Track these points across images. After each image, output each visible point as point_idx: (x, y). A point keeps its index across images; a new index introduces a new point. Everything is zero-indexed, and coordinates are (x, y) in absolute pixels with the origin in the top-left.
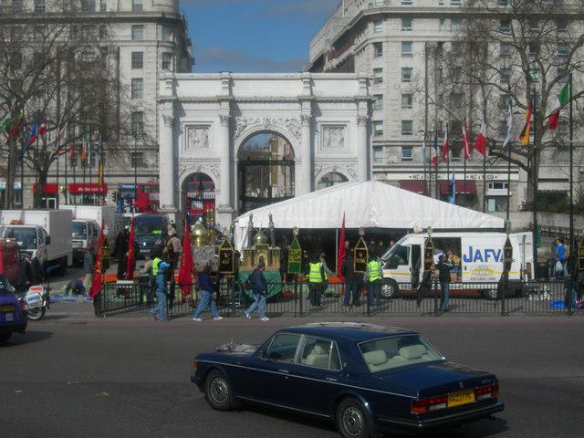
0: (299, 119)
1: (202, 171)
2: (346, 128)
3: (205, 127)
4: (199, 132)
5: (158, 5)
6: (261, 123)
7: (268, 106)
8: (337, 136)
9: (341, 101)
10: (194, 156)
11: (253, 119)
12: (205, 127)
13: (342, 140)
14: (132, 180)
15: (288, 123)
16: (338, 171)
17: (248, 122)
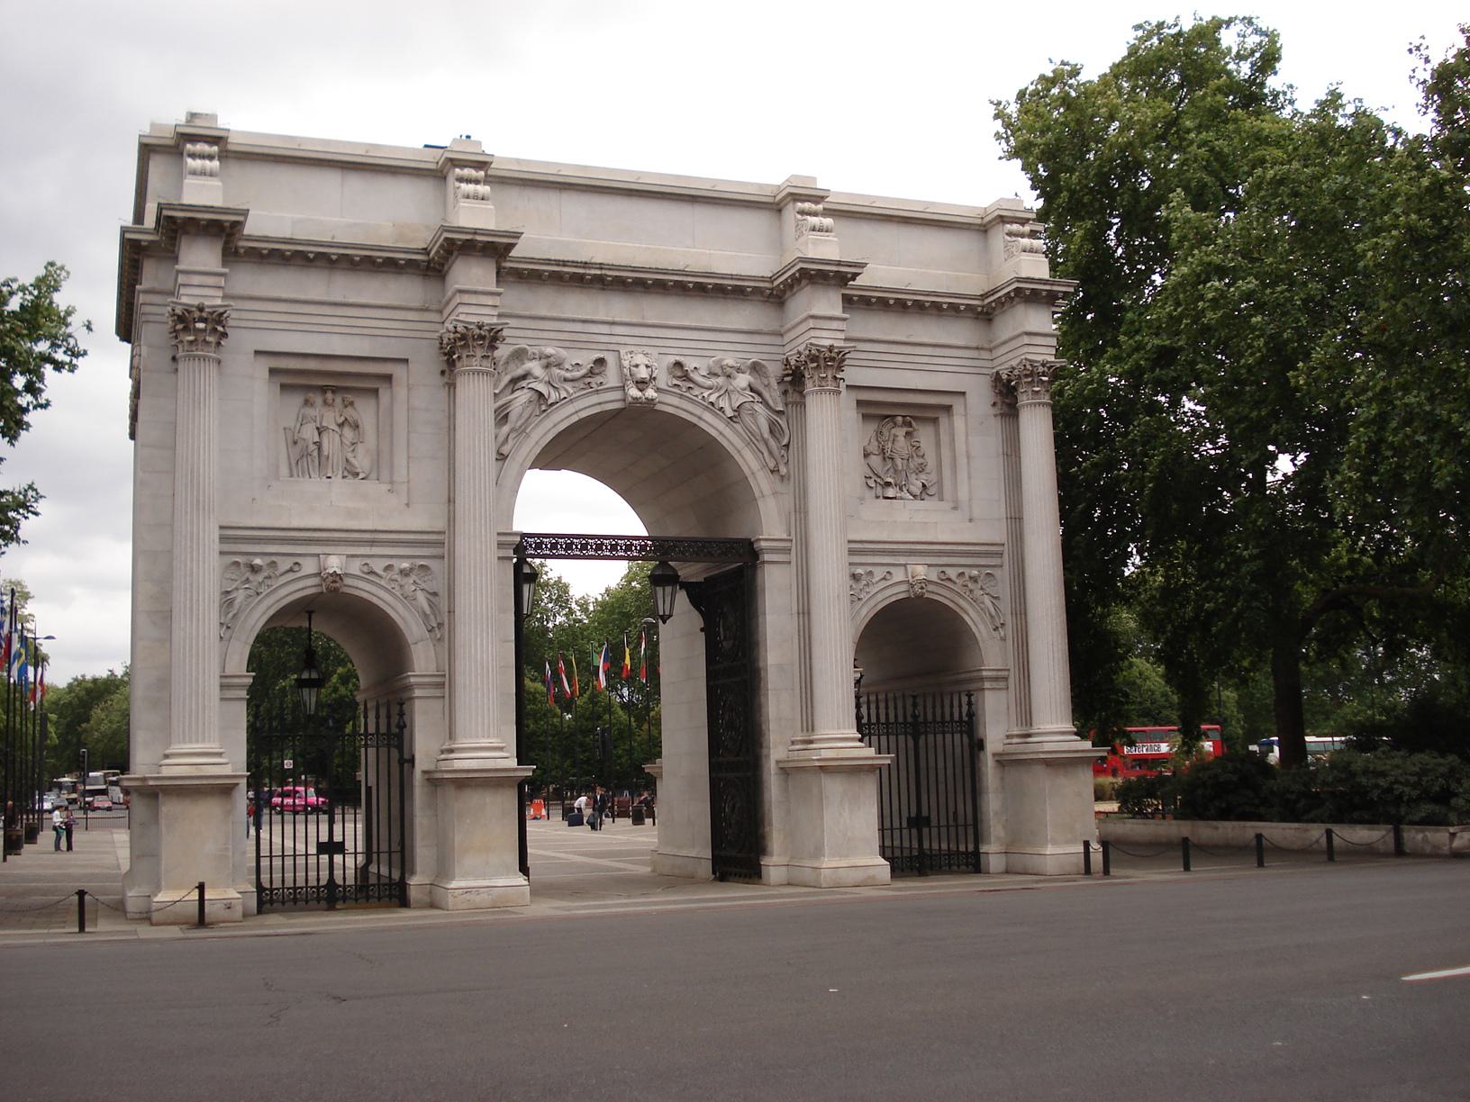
0: (774, 370)
2: (943, 420)
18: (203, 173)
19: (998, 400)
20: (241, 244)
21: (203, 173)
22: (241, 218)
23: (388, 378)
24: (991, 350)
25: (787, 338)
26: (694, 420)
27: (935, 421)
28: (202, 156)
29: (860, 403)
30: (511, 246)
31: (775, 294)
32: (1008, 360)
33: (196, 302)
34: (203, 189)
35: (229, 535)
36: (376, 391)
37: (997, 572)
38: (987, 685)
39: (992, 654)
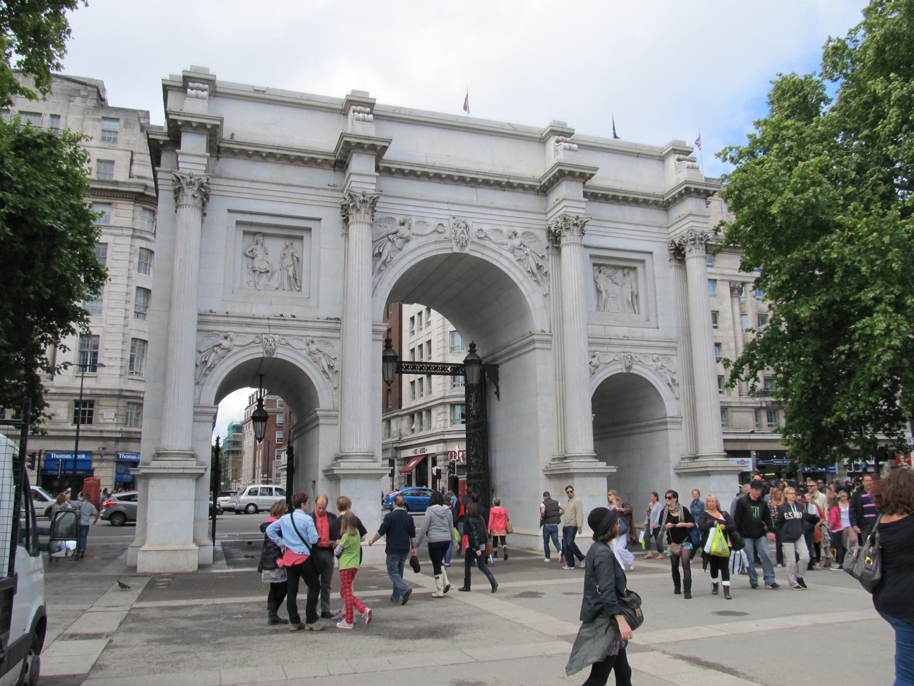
1: (281, 353)
3: (294, 233)
4: (275, 247)
5: (139, 177)
6: (447, 234)
7: (465, 194)
8: (618, 289)
9: (636, 202)
10: (260, 310)
11: (433, 223)
12: (294, 233)
13: (635, 297)
14: (71, 446)
15: (516, 242)
16: (637, 369)
17: (415, 229)
18: (197, 97)
19: (673, 257)
20: (221, 145)
21: (197, 97)
22: (218, 123)
23: (309, 230)
24: (668, 228)
25: (550, 215)
26: (494, 263)
27: (634, 269)
28: (198, 89)
29: (591, 256)
30: (385, 148)
31: (544, 190)
32: (679, 232)
33: (188, 172)
34: (195, 106)
35: (203, 318)
36: (302, 238)
37: (674, 359)
38: (669, 426)
39: (672, 406)
